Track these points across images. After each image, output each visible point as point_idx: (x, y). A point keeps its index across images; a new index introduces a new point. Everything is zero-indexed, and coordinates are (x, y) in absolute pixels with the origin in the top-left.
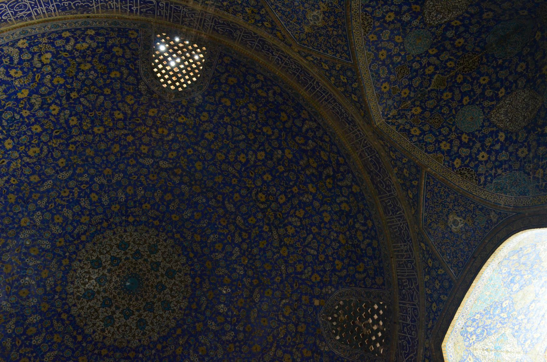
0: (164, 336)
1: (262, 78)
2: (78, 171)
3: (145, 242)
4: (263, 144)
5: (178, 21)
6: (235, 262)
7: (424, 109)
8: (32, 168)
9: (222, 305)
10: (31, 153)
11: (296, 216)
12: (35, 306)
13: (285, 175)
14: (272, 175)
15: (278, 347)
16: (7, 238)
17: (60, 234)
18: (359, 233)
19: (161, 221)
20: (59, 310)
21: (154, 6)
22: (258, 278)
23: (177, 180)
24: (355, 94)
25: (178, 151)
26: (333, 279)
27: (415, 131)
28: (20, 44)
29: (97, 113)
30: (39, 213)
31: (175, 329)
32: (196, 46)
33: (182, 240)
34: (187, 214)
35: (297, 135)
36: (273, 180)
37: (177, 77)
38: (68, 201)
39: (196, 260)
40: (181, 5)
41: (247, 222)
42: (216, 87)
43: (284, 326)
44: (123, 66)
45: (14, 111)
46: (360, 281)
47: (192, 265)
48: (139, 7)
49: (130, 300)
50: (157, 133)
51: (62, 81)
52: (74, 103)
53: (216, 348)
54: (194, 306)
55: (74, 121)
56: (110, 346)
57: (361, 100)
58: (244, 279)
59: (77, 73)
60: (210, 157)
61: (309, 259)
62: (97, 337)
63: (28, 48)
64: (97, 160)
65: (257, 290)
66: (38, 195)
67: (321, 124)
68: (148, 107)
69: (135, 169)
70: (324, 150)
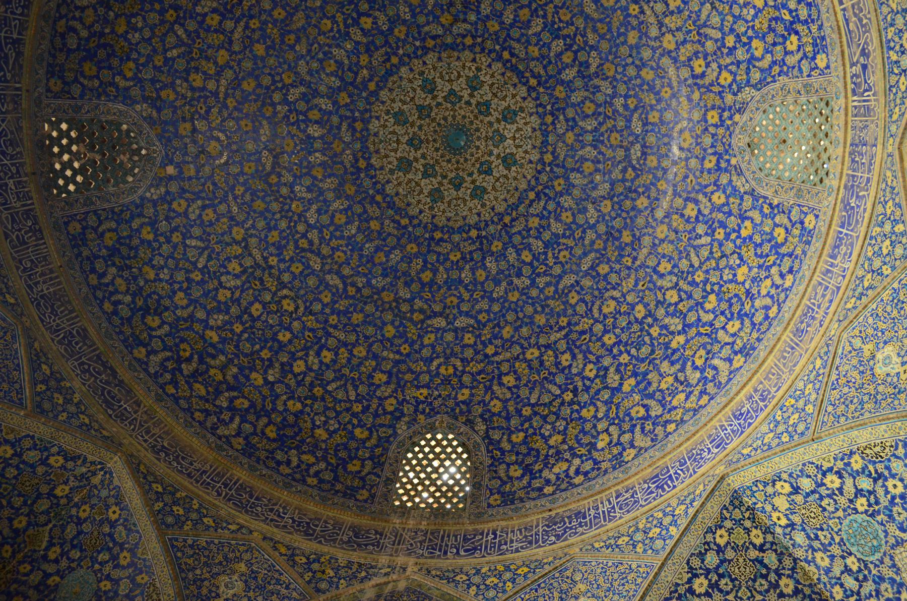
0: (391, 75)
1: (309, 480)
2: (552, 289)
3: (449, 203)
4: (299, 384)
5: (432, 533)
7: (51, 494)
8: (609, 283)
9: (316, 135)
10: (613, 304)
11: (230, 289)
12: (573, 91)
13: (257, 347)
14: (278, 341)
15: (216, 94)
16: (624, 180)
17: (561, 196)
18: (123, 288)
19: (432, 238)
20: (541, 90)
22: (270, 185)
23: (418, 303)
24: (157, 492)
25: (423, 346)
26: (152, 210)
27: (56, 461)
28: (633, 452)
31: (379, 88)
32: (409, 504)
33: (397, 218)
34: (396, 256)
35: (247, 410)
36: (276, 334)
37: (434, 453)
38: (559, 244)
39: (371, 192)
41: (303, 264)
42: (378, 451)
43: (214, 125)
45: (637, 359)
46: (107, 218)
47: (375, 184)
49: (454, 117)
50: (454, 366)
51: (584, 413)
52: (567, 384)
53: (310, 72)
54: (359, 126)
56: (464, 50)
57: (147, 487)
58: (291, 179)
59: (566, 428)
60: (375, 346)
61: (197, 231)
62: (484, 60)
63: (624, 449)
64: (529, 310)
65: (268, 168)
66: (596, 247)
67: (209, 435)
68: (471, 401)
69: (477, 307)
70: (201, 398)
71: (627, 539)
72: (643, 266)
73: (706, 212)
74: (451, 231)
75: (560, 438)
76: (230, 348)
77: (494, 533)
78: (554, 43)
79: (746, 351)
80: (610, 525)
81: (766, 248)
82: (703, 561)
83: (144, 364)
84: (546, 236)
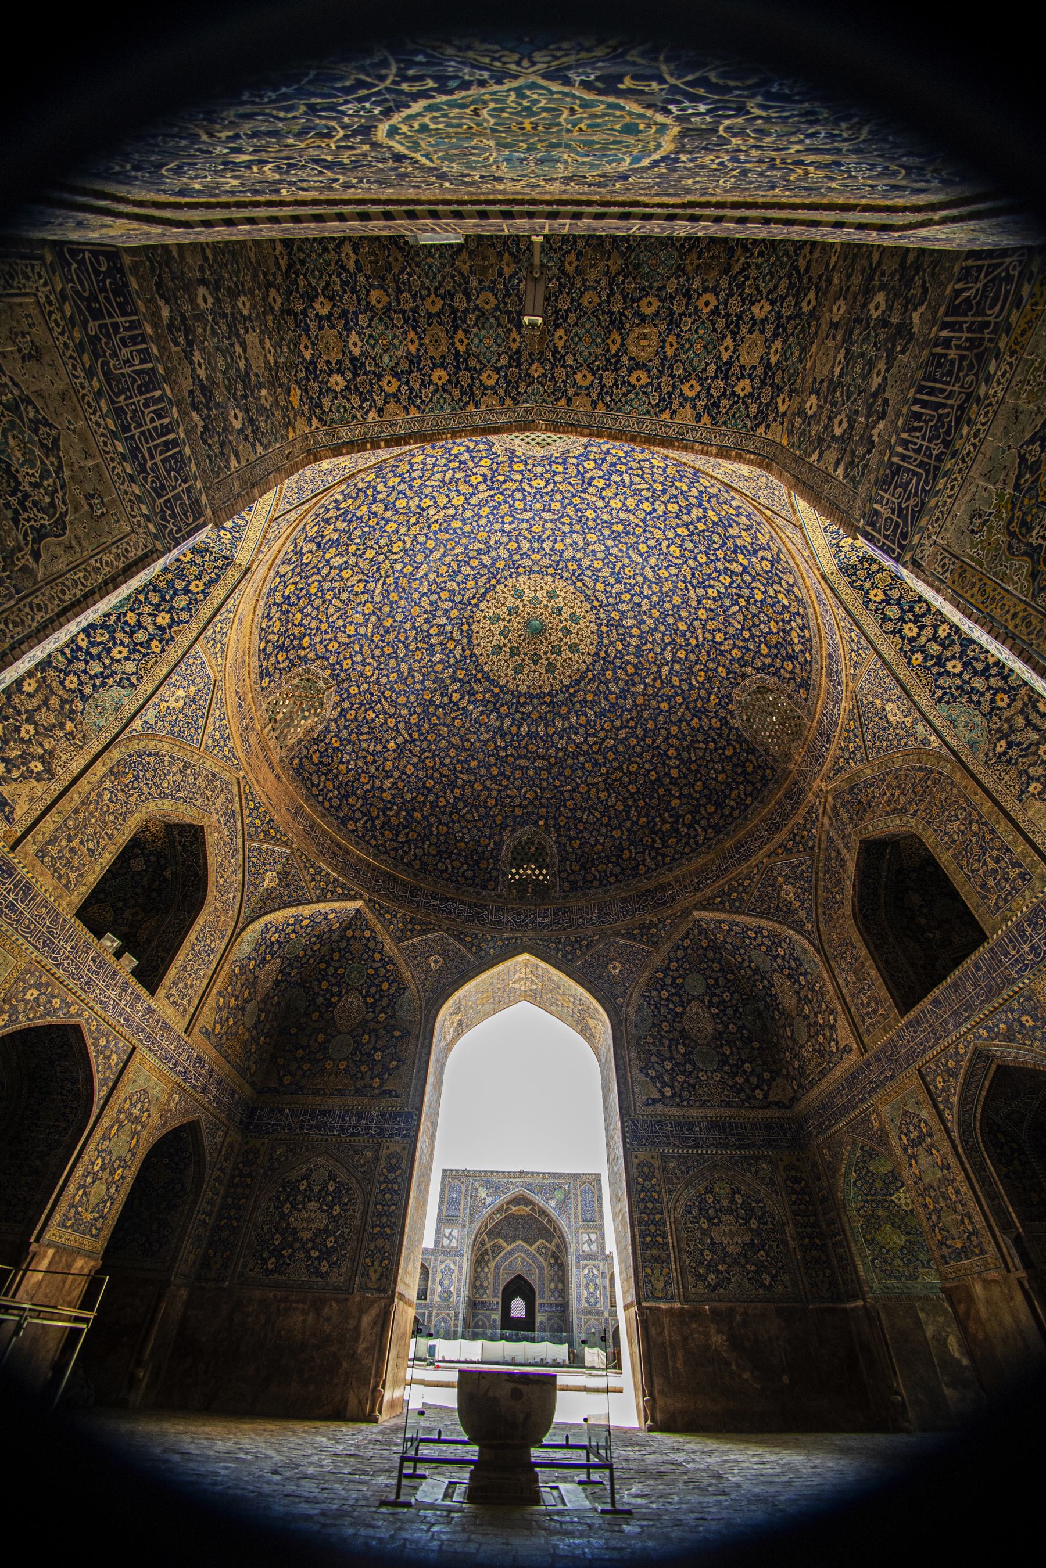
1: (748, 802)
4: (685, 777)
6: (569, 738)
10: (672, 548)
15: (499, 791)
16: (571, 524)
25: (680, 687)
30: (603, 548)
42: (744, 746)
53: (488, 732)
61: (579, 814)
62: (478, 615)
72: (644, 521)
74: (600, 643)
75: (772, 624)
76: (652, 812)
82: (891, 620)
83: (649, 870)
84: (612, 580)
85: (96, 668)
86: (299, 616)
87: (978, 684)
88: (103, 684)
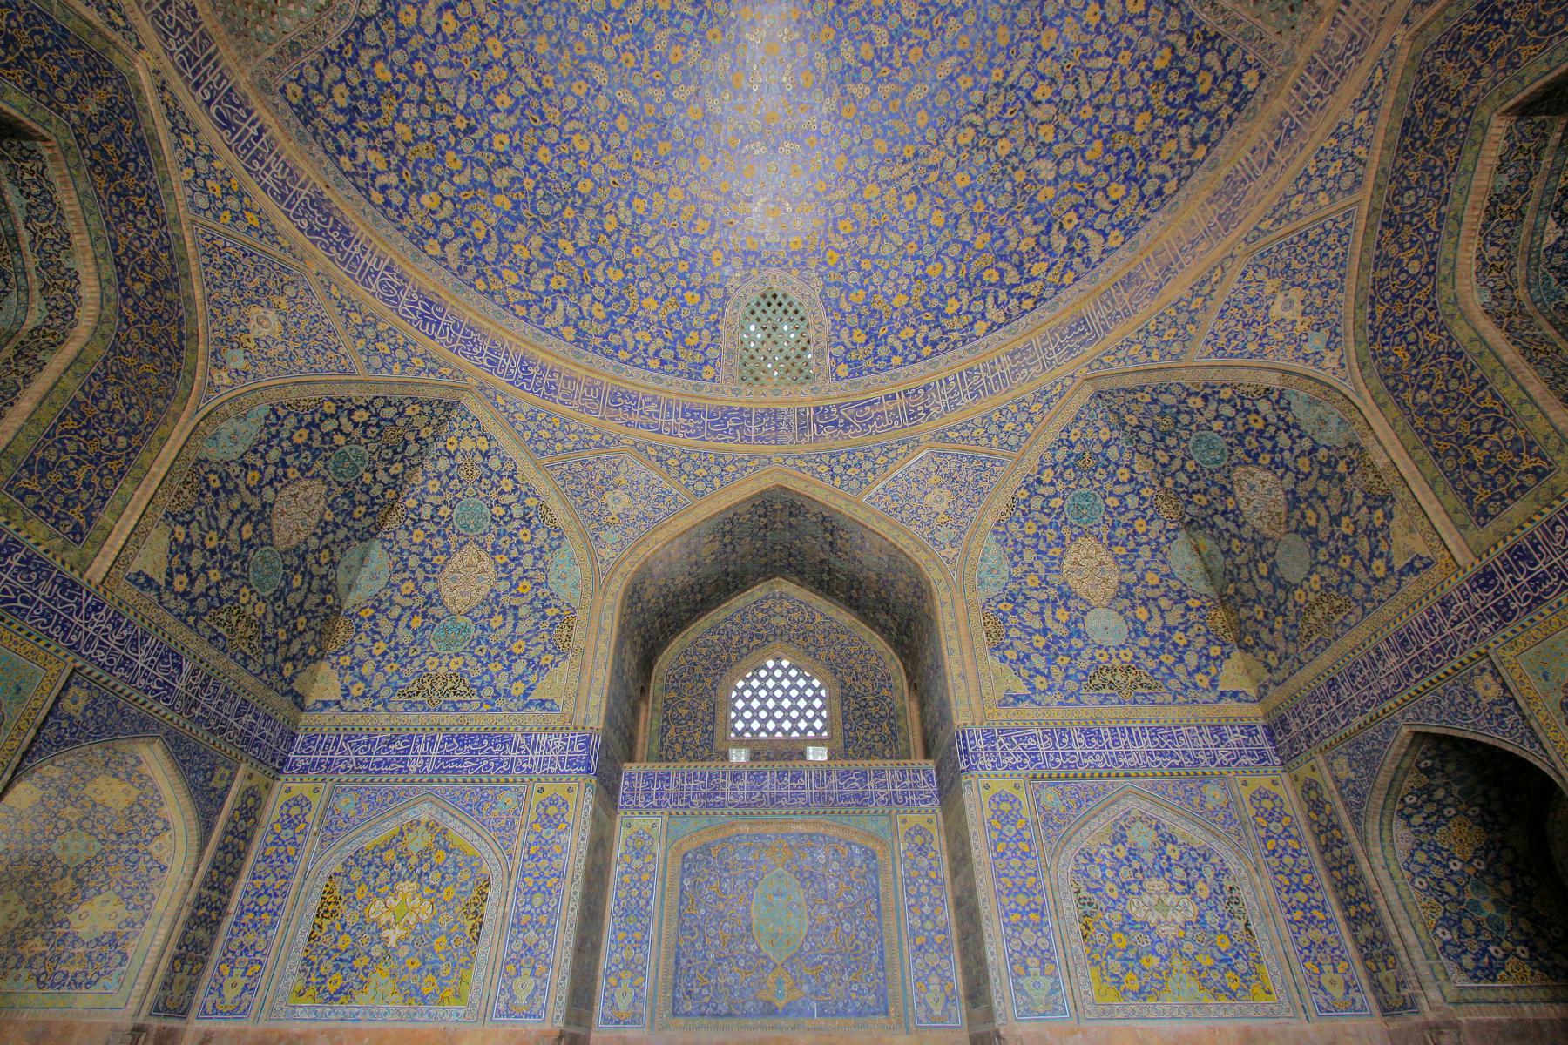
2: (584, 53)
5: (203, 35)
10: (585, 148)
17: (701, 41)
21: (219, 103)
28: (436, 251)
29: (467, 66)
38: (641, 49)
40: (173, 63)
44: (359, 69)
45: (534, 202)
48: (245, 125)
51: (451, 155)
55: (503, 101)
59: (422, 139)
63: (435, 236)
64: (549, 24)
66: (646, 106)
71: (360, 321)
73: (703, 246)
75: (408, 137)
77: (261, 130)
78: (884, 33)
79: (581, 339)
80: (360, 288)
81: (678, 326)
85: (1283, 439)
86: (1138, 128)
87: (274, 454)
88: (1296, 427)
